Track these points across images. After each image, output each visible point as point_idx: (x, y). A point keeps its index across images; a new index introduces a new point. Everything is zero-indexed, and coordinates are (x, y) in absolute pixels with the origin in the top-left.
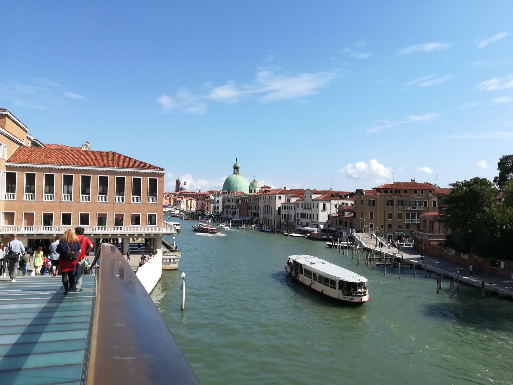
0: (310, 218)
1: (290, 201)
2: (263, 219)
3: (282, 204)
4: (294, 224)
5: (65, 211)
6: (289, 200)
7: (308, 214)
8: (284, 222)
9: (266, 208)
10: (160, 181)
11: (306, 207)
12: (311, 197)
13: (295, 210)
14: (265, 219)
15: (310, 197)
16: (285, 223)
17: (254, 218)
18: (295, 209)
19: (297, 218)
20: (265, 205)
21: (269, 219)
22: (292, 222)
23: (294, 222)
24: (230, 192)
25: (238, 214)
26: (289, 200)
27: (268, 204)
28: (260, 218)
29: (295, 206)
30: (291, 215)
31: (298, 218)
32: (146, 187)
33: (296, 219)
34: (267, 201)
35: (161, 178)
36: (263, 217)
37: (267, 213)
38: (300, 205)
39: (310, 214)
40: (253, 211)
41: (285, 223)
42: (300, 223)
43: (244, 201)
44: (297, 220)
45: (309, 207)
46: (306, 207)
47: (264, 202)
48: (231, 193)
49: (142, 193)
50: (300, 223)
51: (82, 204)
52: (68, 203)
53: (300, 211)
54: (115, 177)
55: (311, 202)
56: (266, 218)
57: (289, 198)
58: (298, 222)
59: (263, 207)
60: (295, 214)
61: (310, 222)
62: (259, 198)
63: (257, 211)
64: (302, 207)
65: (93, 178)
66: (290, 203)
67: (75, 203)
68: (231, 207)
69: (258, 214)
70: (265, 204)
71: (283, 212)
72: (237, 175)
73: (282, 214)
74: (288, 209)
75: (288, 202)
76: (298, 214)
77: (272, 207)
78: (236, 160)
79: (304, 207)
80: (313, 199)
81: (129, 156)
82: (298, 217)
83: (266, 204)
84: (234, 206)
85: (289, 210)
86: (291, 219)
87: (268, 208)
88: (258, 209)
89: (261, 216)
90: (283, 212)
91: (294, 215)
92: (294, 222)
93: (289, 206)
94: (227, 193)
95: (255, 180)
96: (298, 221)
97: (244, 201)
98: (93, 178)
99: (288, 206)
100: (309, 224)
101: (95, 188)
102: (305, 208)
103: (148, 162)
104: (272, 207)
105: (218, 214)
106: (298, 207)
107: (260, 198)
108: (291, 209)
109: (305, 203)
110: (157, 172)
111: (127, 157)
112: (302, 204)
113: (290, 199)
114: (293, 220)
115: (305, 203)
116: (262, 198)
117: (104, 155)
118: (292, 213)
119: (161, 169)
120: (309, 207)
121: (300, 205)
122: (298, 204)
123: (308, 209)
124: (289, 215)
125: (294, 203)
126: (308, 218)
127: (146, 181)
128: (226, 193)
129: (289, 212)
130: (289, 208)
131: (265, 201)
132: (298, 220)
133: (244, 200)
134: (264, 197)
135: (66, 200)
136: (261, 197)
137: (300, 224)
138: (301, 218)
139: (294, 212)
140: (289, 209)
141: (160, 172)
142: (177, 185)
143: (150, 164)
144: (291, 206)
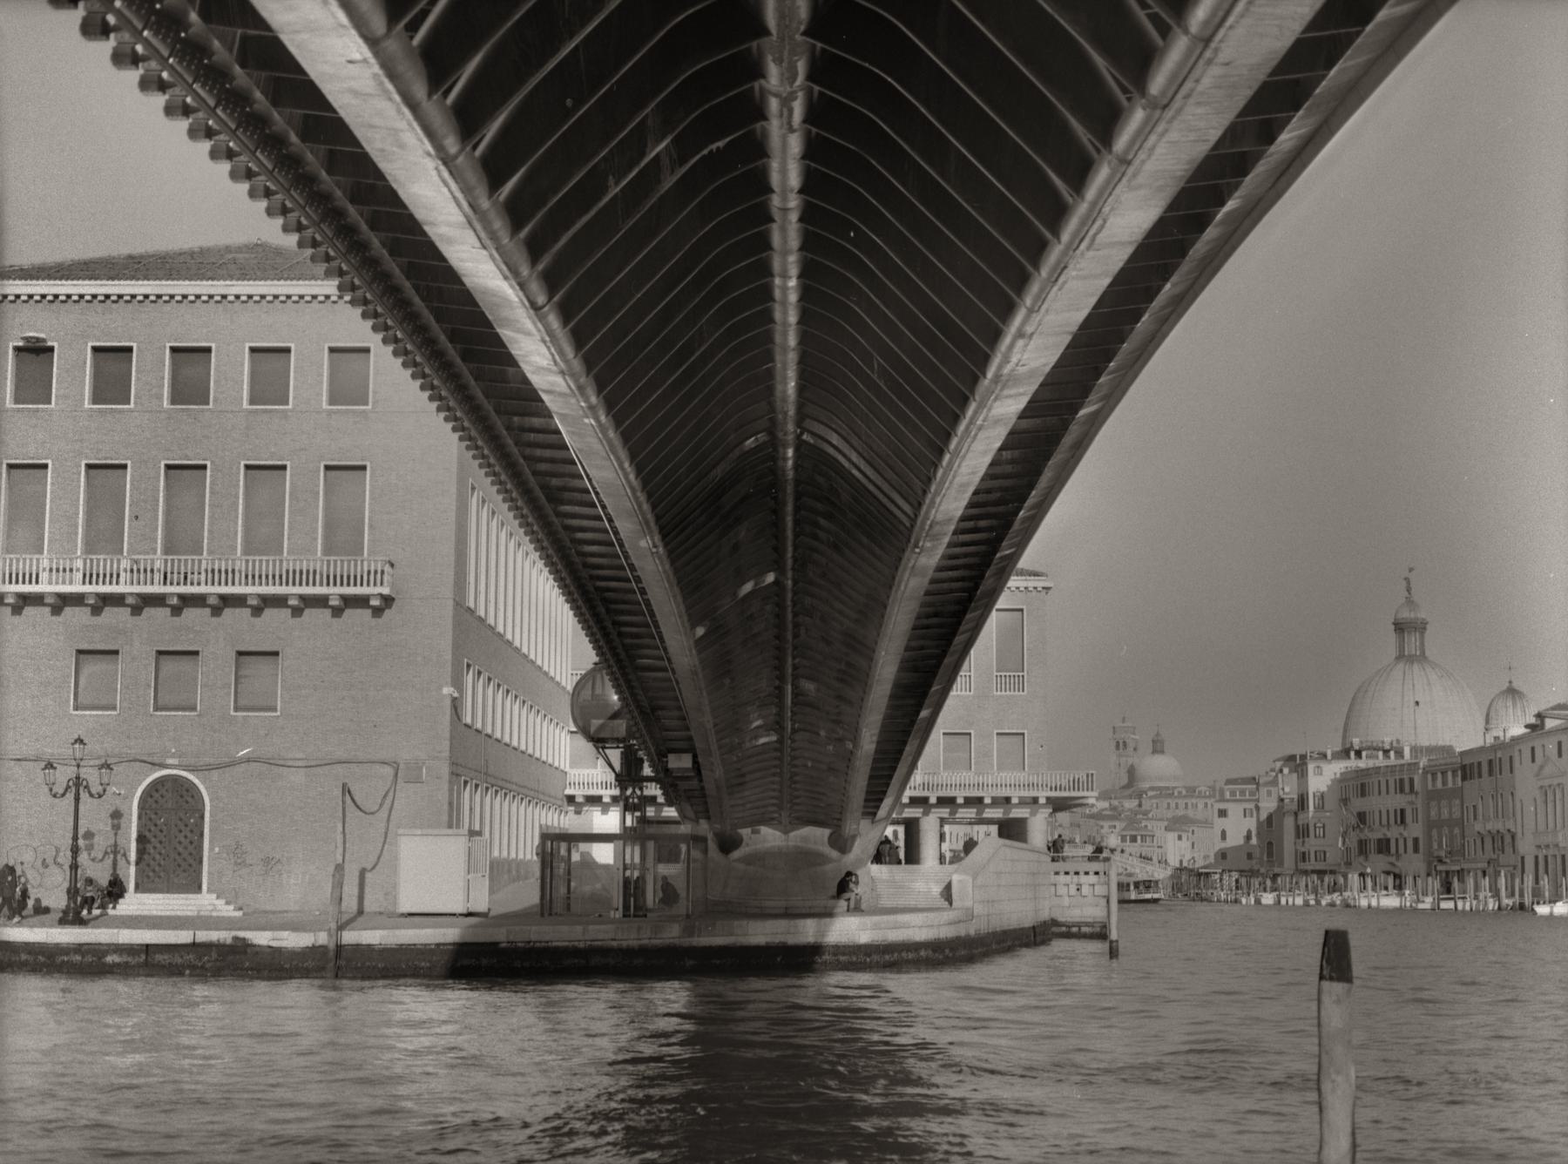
2: (1537, 857)
17: (1497, 860)
20: (1541, 787)
24: (1377, 749)
25: (1416, 850)
27: (1555, 782)
28: (1523, 858)
34: (1547, 770)
36: (1539, 847)
40: (1489, 826)
43: (1444, 783)
47: (1537, 775)
48: (1381, 753)
56: (1551, 852)
59: (1535, 800)
62: (1511, 757)
63: (1510, 825)
68: (1384, 821)
69: (1513, 837)
70: (1540, 783)
72: (1416, 667)
78: (1409, 590)
83: (1546, 783)
84: (1388, 793)
89: (1526, 846)
94: (1364, 754)
95: (1515, 685)
97: (1444, 783)
105: (1320, 866)
107: (1517, 753)
116: (1527, 754)
128: (1358, 754)
131: (1541, 767)
133: (1444, 773)
134: (1533, 749)
136: (1520, 751)
142: (1120, 756)
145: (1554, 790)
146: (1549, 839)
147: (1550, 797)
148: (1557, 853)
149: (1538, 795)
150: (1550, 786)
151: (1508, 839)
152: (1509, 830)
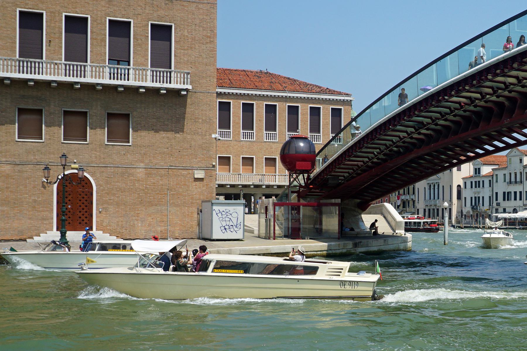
0: (521, 199)
1: (479, 173)
2: (425, 210)
3: (463, 179)
4: (490, 213)
5: (221, 154)
6: (477, 171)
7: (515, 193)
8: (468, 212)
9: (430, 189)
10: (347, 112)
11: (513, 179)
12: (521, 161)
13: (491, 188)
14: (429, 210)
15: (519, 161)
16: (471, 213)
18: (490, 186)
19: (495, 203)
20: (428, 183)
21: (438, 210)
22: (487, 210)
23: (489, 209)
26: (477, 171)
28: (418, 210)
29: (490, 181)
30: (483, 197)
31: (498, 201)
32: (327, 121)
33: (492, 204)
35: (347, 107)
37: (434, 198)
38: (501, 178)
39: (521, 192)
41: (471, 213)
42: (501, 210)
44: (495, 204)
45: (518, 179)
46: (513, 179)
49: (323, 129)
50: (501, 210)
51: (244, 143)
52: (226, 142)
53: (501, 188)
54: (286, 105)
55: (522, 171)
56: (432, 207)
57: (477, 167)
58: (497, 208)
60: (491, 194)
61: (520, 207)
63: (413, 197)
64: (505, 181)
65: (258, 107)
66: (479, 176)
67: (235, 143)
69: (414, 202)
71: (467, 194)
73: (465, 198)
74: (476, 187)
75: (476, 173)
76: (497, 193)
77: (443, 186)
79: (508, 180)
80: (524, 165)
81: (291, 77)
82: (497, 200)
85: (478, 189)
86: (483, 205)
87: (434, 189)
88: (414, 193)
90: (467, 194)
91: (490, 197)
92: (489, 209)
93: (479, 182)
96: (497, 205)
98: (258, 107)
99: (476, 182)
100: (518, 209)
101: (260, 120)
102: (510, 182)
103: (324, 86)
104: (443, 186)
106: (497, 181)
108: (483, 186)
109: (510, 174)
110: (342, 98)
111: (289, 78)
112: (505, 175)
113: (479, 169)
114: (488, 204)
115: (510, 174)
117: (260, 74)
118: (485, 193)
119: (347, 95)
120: (518, 179)
121: (501, 178)
122: (497, 175)
123: (516, 182)
124: (479, 197)
125: (488, 175)
126: (515, 199)
127: (327, 111)
129: (479, 193)
130: (477, 184)
132: (498, 204)
135: (224, 138)
137: (502, 211)
138: (504, 200)
139: (490, 191)
140: (479, 187)
141: (346, 98)
143: (327, 88)
144: (483, 181)
145: (434, 186)
146: (433, 203)
147: (432, 187)
148: (435, 208)
149: (427, 188)
150: (432, 183)
151: (411, 203)
152: (412, 199)
